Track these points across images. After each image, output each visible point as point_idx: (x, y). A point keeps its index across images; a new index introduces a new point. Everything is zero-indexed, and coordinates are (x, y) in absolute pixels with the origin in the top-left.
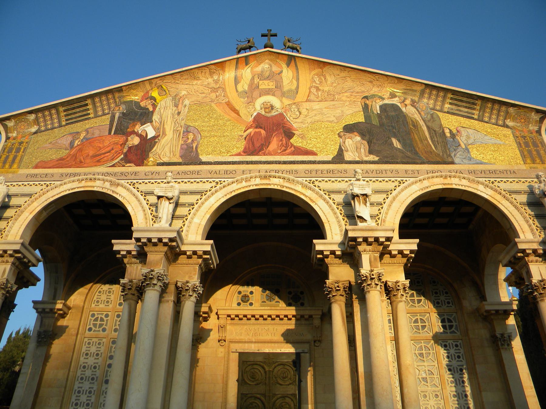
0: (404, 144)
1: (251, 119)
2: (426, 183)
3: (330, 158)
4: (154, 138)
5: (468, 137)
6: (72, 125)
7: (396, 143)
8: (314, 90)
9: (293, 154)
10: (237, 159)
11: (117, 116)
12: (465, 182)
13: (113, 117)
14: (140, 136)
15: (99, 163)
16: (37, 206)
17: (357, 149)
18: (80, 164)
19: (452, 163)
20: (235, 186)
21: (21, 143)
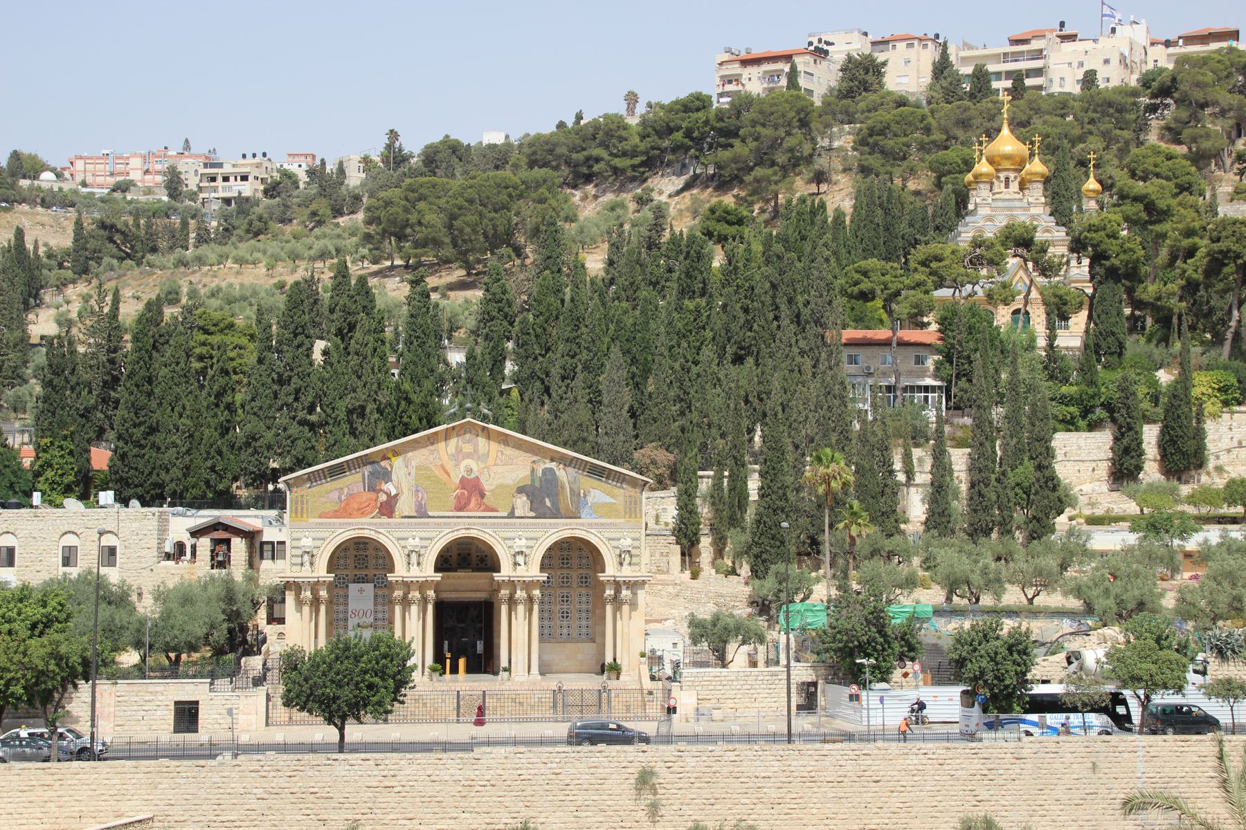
0: (552, 503)
1: (457, 481)
2: (560, 533)
3: (505, 514)
4: (396, 495)
5: (594, 497)
6: (335, 482)
7: (548, 503)
8: (499, 454)
9: (484, 510)
10: (451, 514)
11: (366, 474)
12: (584, 533)
13: (364, 474)
14: (386, 493)
15: (363, 514)
16: (331, 548)
17: (524, 506)
18: (350, 516)
19: (580, 518)
20: (451, 535)
21: (302, 496)
